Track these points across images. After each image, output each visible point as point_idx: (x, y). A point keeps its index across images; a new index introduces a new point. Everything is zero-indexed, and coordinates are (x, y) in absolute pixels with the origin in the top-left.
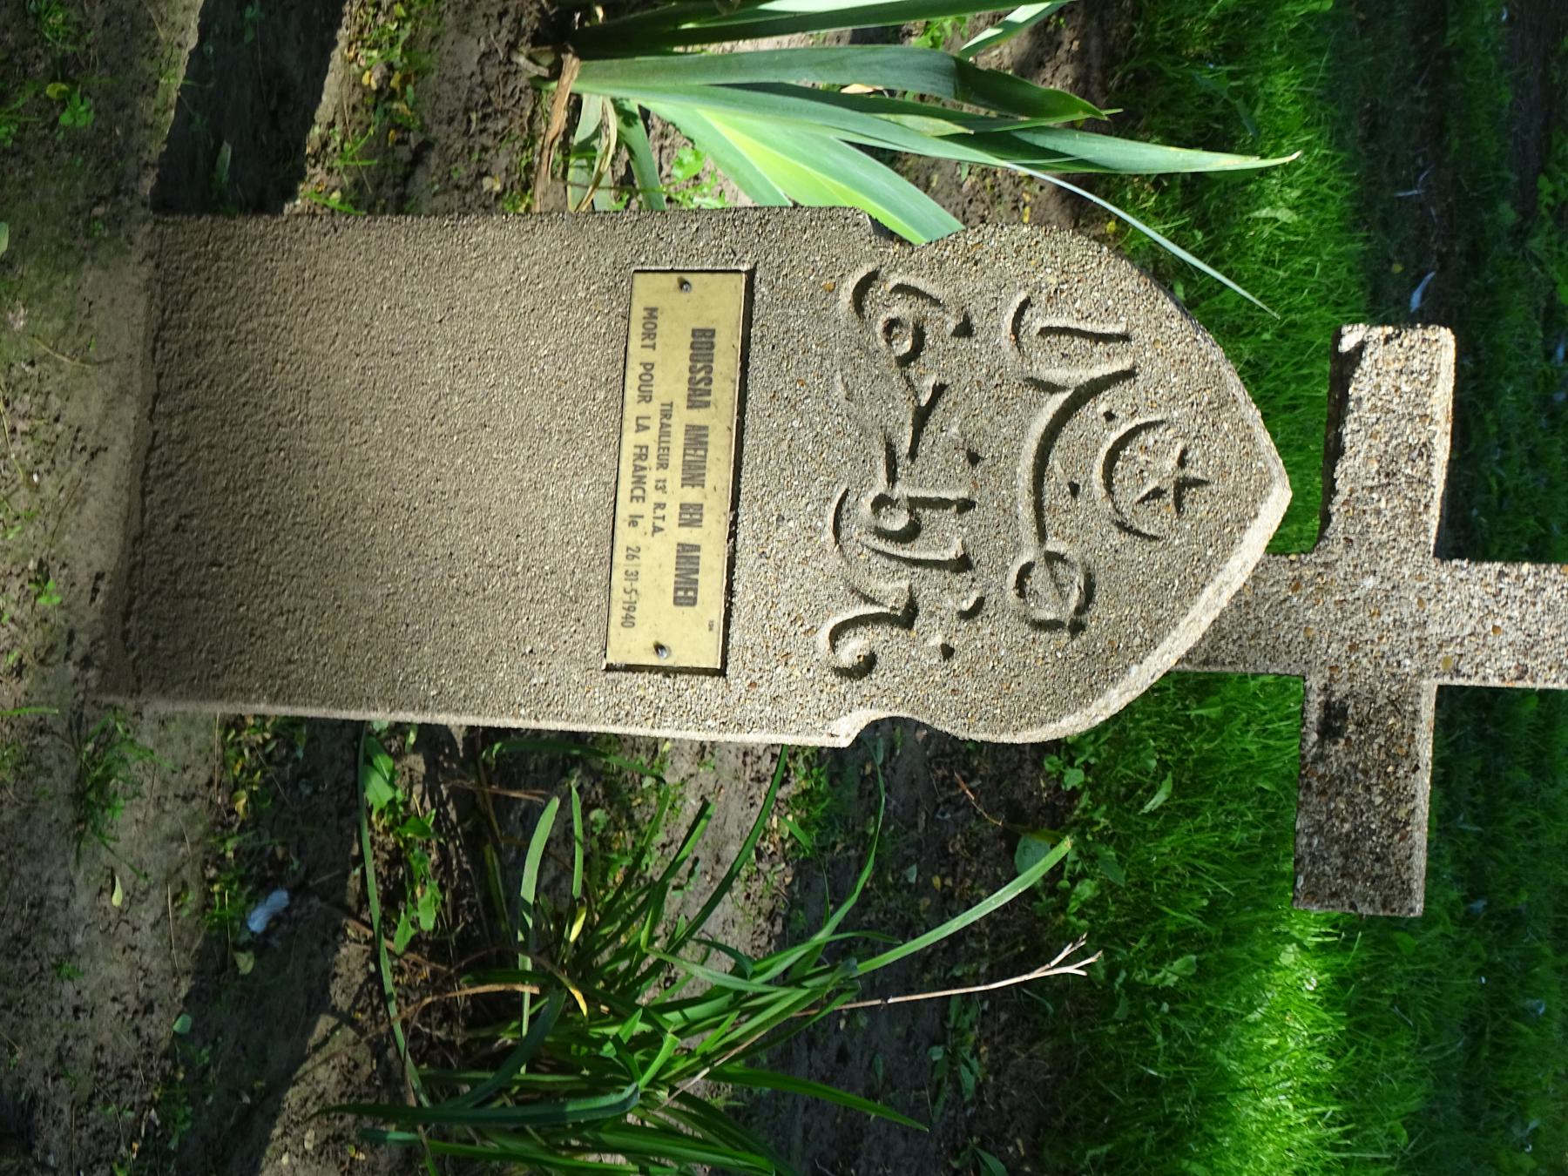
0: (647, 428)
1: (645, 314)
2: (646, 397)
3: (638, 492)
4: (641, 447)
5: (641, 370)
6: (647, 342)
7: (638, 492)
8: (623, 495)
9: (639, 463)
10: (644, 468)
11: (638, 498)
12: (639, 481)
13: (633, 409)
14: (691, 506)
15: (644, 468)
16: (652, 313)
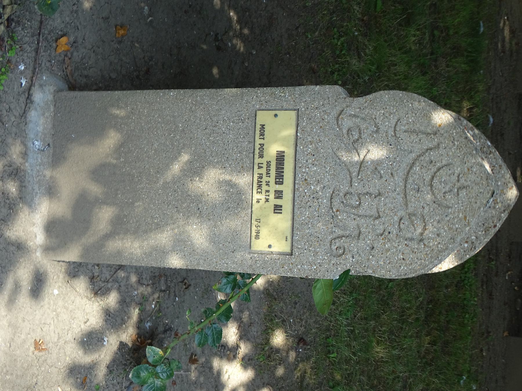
0: (262, 167)
1: (260, 127)
2: (261, 156)
3: (259, 190)
4: (260, 174)
5: (259, 146)
6: (261, 137)
7: (259, 190)
8: (255, 191)
9: (259, 180)
10: (261, 182)
11: (259, 192)
12: (260, 186)
13: (257, 160)
14: (279, 191)
15: (261, 182)
16: (263, 126)
